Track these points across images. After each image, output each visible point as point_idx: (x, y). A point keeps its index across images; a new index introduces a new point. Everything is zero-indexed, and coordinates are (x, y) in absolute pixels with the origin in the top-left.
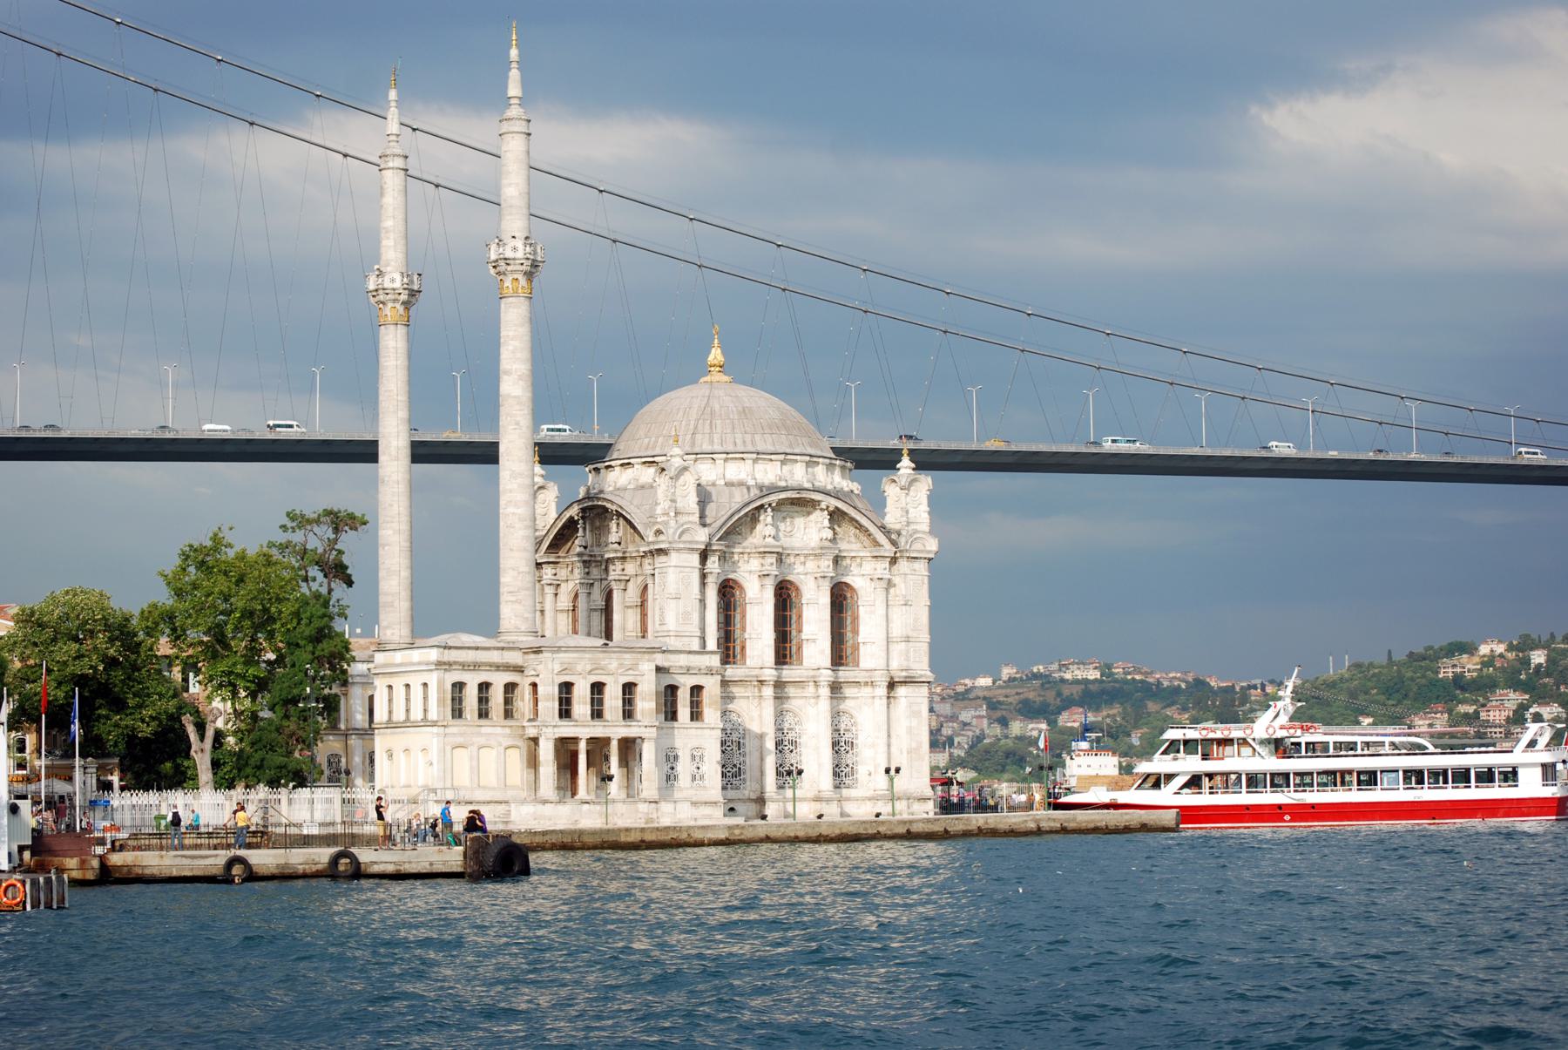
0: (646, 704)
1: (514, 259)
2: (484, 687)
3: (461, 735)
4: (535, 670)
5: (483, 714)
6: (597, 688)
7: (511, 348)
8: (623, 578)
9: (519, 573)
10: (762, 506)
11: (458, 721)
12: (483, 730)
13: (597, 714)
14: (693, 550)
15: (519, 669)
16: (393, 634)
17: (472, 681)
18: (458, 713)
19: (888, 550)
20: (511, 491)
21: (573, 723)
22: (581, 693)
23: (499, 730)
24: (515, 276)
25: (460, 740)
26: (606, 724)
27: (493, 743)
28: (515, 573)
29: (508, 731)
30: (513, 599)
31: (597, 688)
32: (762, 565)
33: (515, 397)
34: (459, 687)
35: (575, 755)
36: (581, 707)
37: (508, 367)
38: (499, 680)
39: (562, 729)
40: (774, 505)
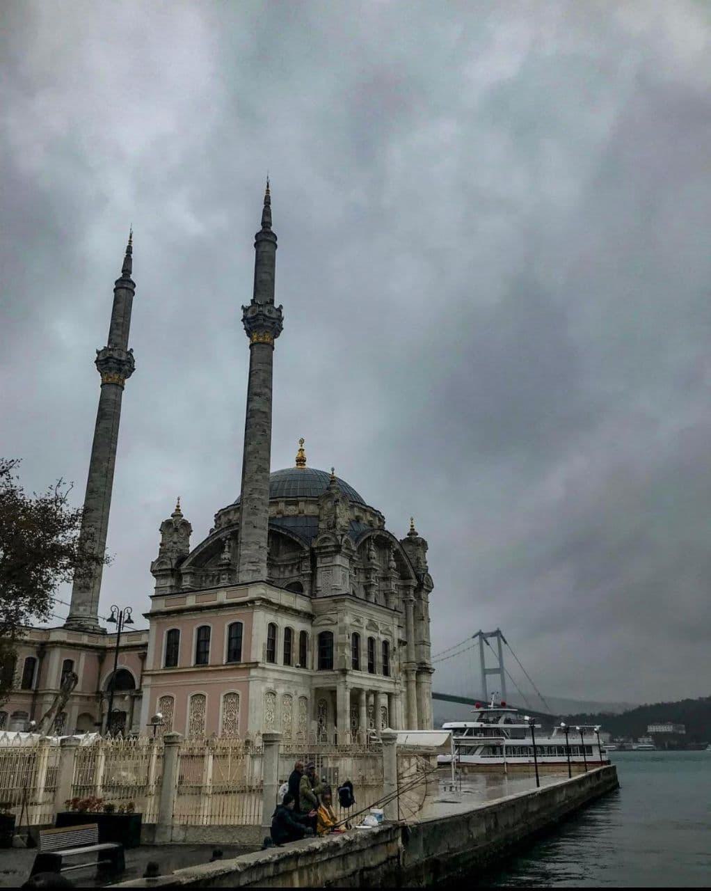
2: (289, 631)
5: (287, 661)
6: (371, 640)
7: (261, 378)
8: (271, 579)
9: (260, 547)
10: (369, 538)
15: (309, 617)
16: (85, 610)
19: (414, 583)
20: (257, 481)
22: (364, 644)
24: (268, 331)
27: (292, 691)
28: (257, 547)
30: (255, 568)
32: (367, 578)
33: (264, 412)
34: (273, 627)
36: (364, 661)
37: (259, 391)
39: (354, 680)
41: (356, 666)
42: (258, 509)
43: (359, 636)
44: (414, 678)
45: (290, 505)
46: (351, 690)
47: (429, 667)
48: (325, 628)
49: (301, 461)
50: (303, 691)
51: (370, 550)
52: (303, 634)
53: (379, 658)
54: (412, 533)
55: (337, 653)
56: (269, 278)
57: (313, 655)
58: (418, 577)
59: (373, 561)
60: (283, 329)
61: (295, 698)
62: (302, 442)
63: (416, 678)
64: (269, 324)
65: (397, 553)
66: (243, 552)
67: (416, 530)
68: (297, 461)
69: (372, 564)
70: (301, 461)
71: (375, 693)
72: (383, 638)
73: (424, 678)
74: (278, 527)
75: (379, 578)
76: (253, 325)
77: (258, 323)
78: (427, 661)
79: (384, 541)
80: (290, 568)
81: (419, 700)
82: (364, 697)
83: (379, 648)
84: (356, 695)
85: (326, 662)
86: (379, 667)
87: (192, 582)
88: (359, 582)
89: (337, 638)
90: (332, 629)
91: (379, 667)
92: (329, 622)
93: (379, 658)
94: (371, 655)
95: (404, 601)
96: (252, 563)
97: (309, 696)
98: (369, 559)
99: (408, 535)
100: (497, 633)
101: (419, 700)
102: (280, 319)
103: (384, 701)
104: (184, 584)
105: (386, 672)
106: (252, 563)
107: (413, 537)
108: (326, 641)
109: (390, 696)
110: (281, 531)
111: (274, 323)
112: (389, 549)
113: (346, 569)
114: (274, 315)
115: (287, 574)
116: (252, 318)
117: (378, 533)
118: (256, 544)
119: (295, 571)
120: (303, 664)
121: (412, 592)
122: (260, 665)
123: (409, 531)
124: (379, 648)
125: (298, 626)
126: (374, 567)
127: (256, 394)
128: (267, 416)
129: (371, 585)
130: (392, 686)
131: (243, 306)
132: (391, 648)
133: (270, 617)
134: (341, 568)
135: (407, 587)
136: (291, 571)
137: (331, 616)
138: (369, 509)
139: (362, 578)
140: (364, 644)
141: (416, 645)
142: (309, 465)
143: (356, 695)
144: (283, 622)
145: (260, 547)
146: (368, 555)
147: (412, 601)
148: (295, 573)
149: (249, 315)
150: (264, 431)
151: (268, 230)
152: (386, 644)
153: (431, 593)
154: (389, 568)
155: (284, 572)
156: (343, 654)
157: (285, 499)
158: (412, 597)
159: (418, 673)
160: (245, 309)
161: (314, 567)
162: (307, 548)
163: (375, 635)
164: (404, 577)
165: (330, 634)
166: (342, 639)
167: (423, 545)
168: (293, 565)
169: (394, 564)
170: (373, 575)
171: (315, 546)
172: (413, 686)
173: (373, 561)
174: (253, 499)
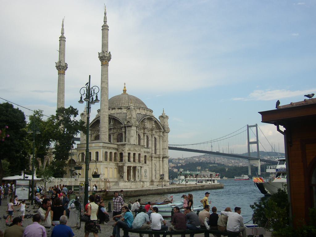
0: (142, 159)
2: (111, 153)
3: (106, 165)
4: (122, 149)
5: (111, 160)
6: (134, 154)
11: (107, 162)
12: (111, 164)
13: (134, 161)
14: (136, 126)
17: (109, 151)
18: (106, 159)
19: (162, 130)
22: (132, 155)
23: (113, 164)
25: (106, 166)
27: (112, 167)
29: (115, 164)
31: (134, 154)
34: (106, 152)
35: (131, 170)
36: (132, 159)
37: (104, 81)
38: (114, 151)
39: (129, 164)
41: (129, 161)
44: (161, 159)
48: (121, 152)
49: (125, 91)
52: (115, 153)
53: (137, 158)
55: (124, 158)
56: (106, 42)
58: (164, 129)
59: (146, 126)
62: (125, 84)
63: (162, 159)
64: (106, 59)
66: (101, 129)
70: (125, 91)
72: (139, 153)
73: (165, 159)
74: (115, 117)
76: (102, 59)
78: (166, 154)
79: (151, 119)
81: (163, 165)
82: (132, 168)
83: (137, 156)
84: (129, 168)
85: (121, 160)
89: (124, 154)
90: (123, 152)
93: (137, 158)
94: (134, 158)
97: (117, 167)
98: (145, 125)
101: (163, 165)
105: (139, 161)
107: (164, 115)
108: (121, 154)
109: (141, 167)
111: (108, 58)
112: (153, 121)
114: (108, 56)
115: (119, 131)
116: (101, 57)
118: (105, 127)
119: (121, 130)
121: (161, 133)
124: (137, 156)
127: (103, 82)
128: (107, 89)
130: (142, 165)
134: (133, 130)
136: (120, 130)
137: (123, 149)
140: (132, 155)
141: (163, 149)
142: (127, 92)
143: (129, 168)
144: (109, 151)
148: (121, 130)
149: (100, 56)
150: (106, 94)
152: (139, 154)
155: (117, 130)
156: (126, 158)
159: (163, 158)
160: (99, 54)
161: (125, 130)
162: (123, 124)
163: (135, 152)
166: (126, 154)
167: (167, 117)
169: (154, 126)
170: (146, 130)
171: (126, 124)
172: (161, 162)
173: (146, 126)
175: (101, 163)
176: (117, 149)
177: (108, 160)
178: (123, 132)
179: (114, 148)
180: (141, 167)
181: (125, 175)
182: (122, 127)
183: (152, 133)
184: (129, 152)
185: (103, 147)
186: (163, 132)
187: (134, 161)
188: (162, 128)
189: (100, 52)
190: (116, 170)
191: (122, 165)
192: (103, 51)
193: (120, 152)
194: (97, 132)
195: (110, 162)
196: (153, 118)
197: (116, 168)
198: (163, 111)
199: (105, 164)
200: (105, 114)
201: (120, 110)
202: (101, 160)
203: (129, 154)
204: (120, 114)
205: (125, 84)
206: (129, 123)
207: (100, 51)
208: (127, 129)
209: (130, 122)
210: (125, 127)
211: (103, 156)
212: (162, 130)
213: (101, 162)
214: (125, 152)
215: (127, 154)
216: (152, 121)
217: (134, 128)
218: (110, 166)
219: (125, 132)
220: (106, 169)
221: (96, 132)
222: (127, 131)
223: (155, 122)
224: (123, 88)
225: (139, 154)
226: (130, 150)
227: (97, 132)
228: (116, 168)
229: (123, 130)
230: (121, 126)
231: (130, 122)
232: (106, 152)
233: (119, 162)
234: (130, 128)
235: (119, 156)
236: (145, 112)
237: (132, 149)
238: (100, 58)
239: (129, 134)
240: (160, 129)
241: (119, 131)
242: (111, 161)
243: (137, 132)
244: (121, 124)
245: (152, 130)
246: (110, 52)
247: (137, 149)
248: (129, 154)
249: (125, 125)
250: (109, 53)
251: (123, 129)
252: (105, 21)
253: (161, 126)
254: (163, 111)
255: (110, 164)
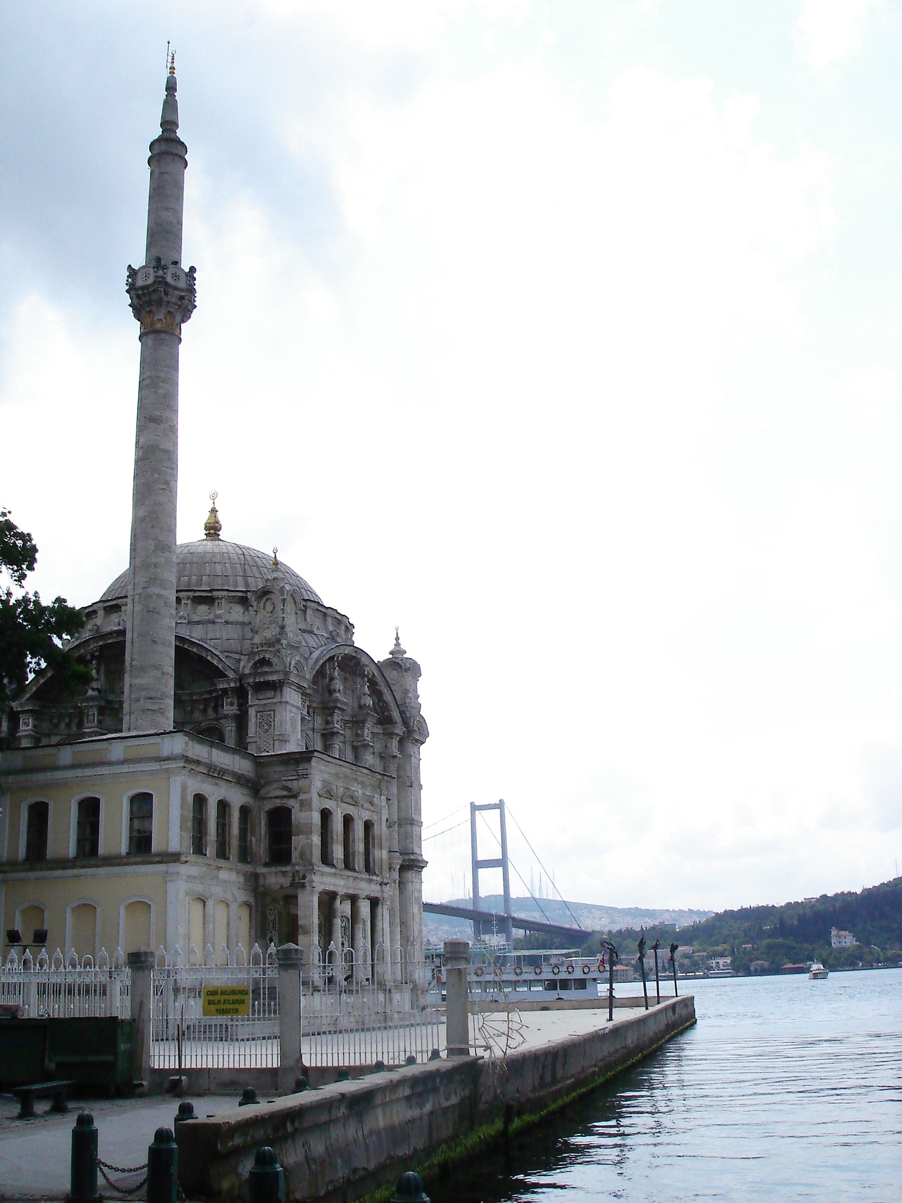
1: (176, 288)
2: (223, 806)
6: (348, 820)
10: (331, 659)
12: (224, 875)
13: (348, 864)
17: (214, 792)
18: (199, 848)
19: (399, 730)
21: (333, 870)
22: (338, 825)
25: (199, 888)
26: (355, 874)
27: (229, 897)
30: (156, 707)
31: (348, 820)
32: (327, 722)
34: (200, 800)
36: (338, 852)
39: (327, 879)
40: (340, 658)
41: (326, 859)
42: (158, 613)
43: (331, 813)
45: (200, 603)
46: (320, 893)
47: (420, 858)
48: (278, 803)
49: (213, 529)
50: (242, 896)
51: (332, 679)
52: (245, 811)
53: (359, 847)
54: (397, 652)
55: (298, 841)
57: (260, 843)
58: (405, 723)
60: (196, 307)
61: (234, 906)
62: (214, 497)
64: (174, 300)
65: (373, 683)
67: (403, 646)
68: (206, 528)
69: (337, 700)
71: (353, 899)
72: (366, 815)
73: (410, 875)
75: (346, 722)
77: (154, 297)
78: (416, 850)
80: (202, 707)
84: (328, 900)
86: (359, 863)
87: (35, 726)
88: (313, 730)
89: (298, 816)
90: (291, 803)
91: (359, 863)
92: (285, 793)
93: (359, 847)
95: (382, 758)
96: (151, 698)
97: (252, 900)
99: (391, 653)
100: (500, 806)
102: (192, 291)
103: (365, 908)
104: (22, 727)
106: (151, 698)
109: (375, 903)
110: (186, 646)
111: (182, 298)
113: (297, 707)
114: (182, 284)
115: (197, 715)
116: (143, 288)
117: (347, 650)
119: (210, 712)
120: (245, 855)
121: (395, 743)
122: (183, 858)
123: (392, 647)
125: (237, 798)
126: (339, 705)
129: (333, 734)
130: (379, 887)
131: (130, 266)
132: (376, 830)
133: (197, 785)
135: (391, 735)
136: (205, 711)
137: (289, 784)
138: (330, 611)
139: (319, 721)
140: (338, 825)
142: (223, 535)
143: (328, 900)
144: (214, 792)
145: (163, 674)
146: (329, 685)
147: (395, 757)
148: (210, 712)
149: (140, 283)
151: (172, 136)
152: (368, 825)
153: (422, 747)
154: (361, 707)
155: (192, 712)
157: (191, 594)
158: (396, 752)
160: (133, 273)
162: (231, 675)
164: (385, 720)
165: (287, 811)
168: (207, 701)
169: (369, 701)
170: (336, 718)
171: (247, 671)
174: (150, 596)
175: (173, 867)
176: (254, 786)
177: (211, 849)
178: (226, 717)
179: (240, 780)
180: (375, 903)
181: (310, 943)
182: (225, 691)
183: (358, 735)
184: (329, 804)
185: (187, 760)
186: (401, 742)
187: (348, 864)
188: (396, 715)
189: (136, 267)
190: (245, 914)
191: (286, 881)
192: (158, 260)
193: (269, 805)
194: (68, 725)
195: (222, 863)
196: (364, 660)
197: (247, 904)
198: (397, 639)
199: (194, 871)
200: (159, 596)
201: (203, 608)
202: (174, 846)
203: (326, 815)
204: (210, 626)
205: (214, 497)
206: (266, 669)
207: (139, 260)
208: (251, 699)
209: (275, 660)
210: (241, 693)
211: (183, 820)
212: (399, 730)
213: (174, 857)
214: (306, 805)
215: (316, 817)
216: (359, 680)
217: (292, 696)
218: (217, 891)
219: (241, 721)
220: (197, 908)
221: (63, 726)
222: (252, 712)
223: (373, 683)
224: (205, 517)
225: (368, 825)
226: (328, 794)
227: (68, 725)
228: (247, 904)
229: (230, 708)
230: (221, 686)
231: (268, 663)
232: (200, 800)
233: (266, 865)
234: (270, 694)
235: (263, 829)
236: (326, 628)
237: (339, 787)
238: (138, 296)
239: (267, 724)
240: (385, 720)
241: (197, 715)
242: (228, 859)
243: (303, 719)
244: (222, 675)
245: (357, 723)
246: (193, 269)
247: (358, 790)
248: (326, 815)
249: (241, 678)
250: (187, 270)
251: (226, 701)
252: (169, 118)
253: (392, 705)
254: (397, 639)
255: (217, 878)
